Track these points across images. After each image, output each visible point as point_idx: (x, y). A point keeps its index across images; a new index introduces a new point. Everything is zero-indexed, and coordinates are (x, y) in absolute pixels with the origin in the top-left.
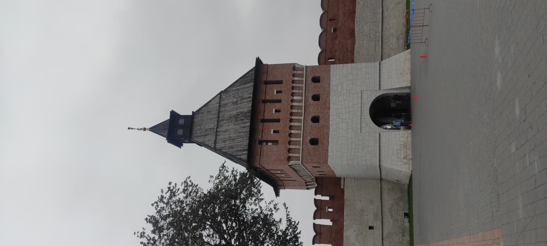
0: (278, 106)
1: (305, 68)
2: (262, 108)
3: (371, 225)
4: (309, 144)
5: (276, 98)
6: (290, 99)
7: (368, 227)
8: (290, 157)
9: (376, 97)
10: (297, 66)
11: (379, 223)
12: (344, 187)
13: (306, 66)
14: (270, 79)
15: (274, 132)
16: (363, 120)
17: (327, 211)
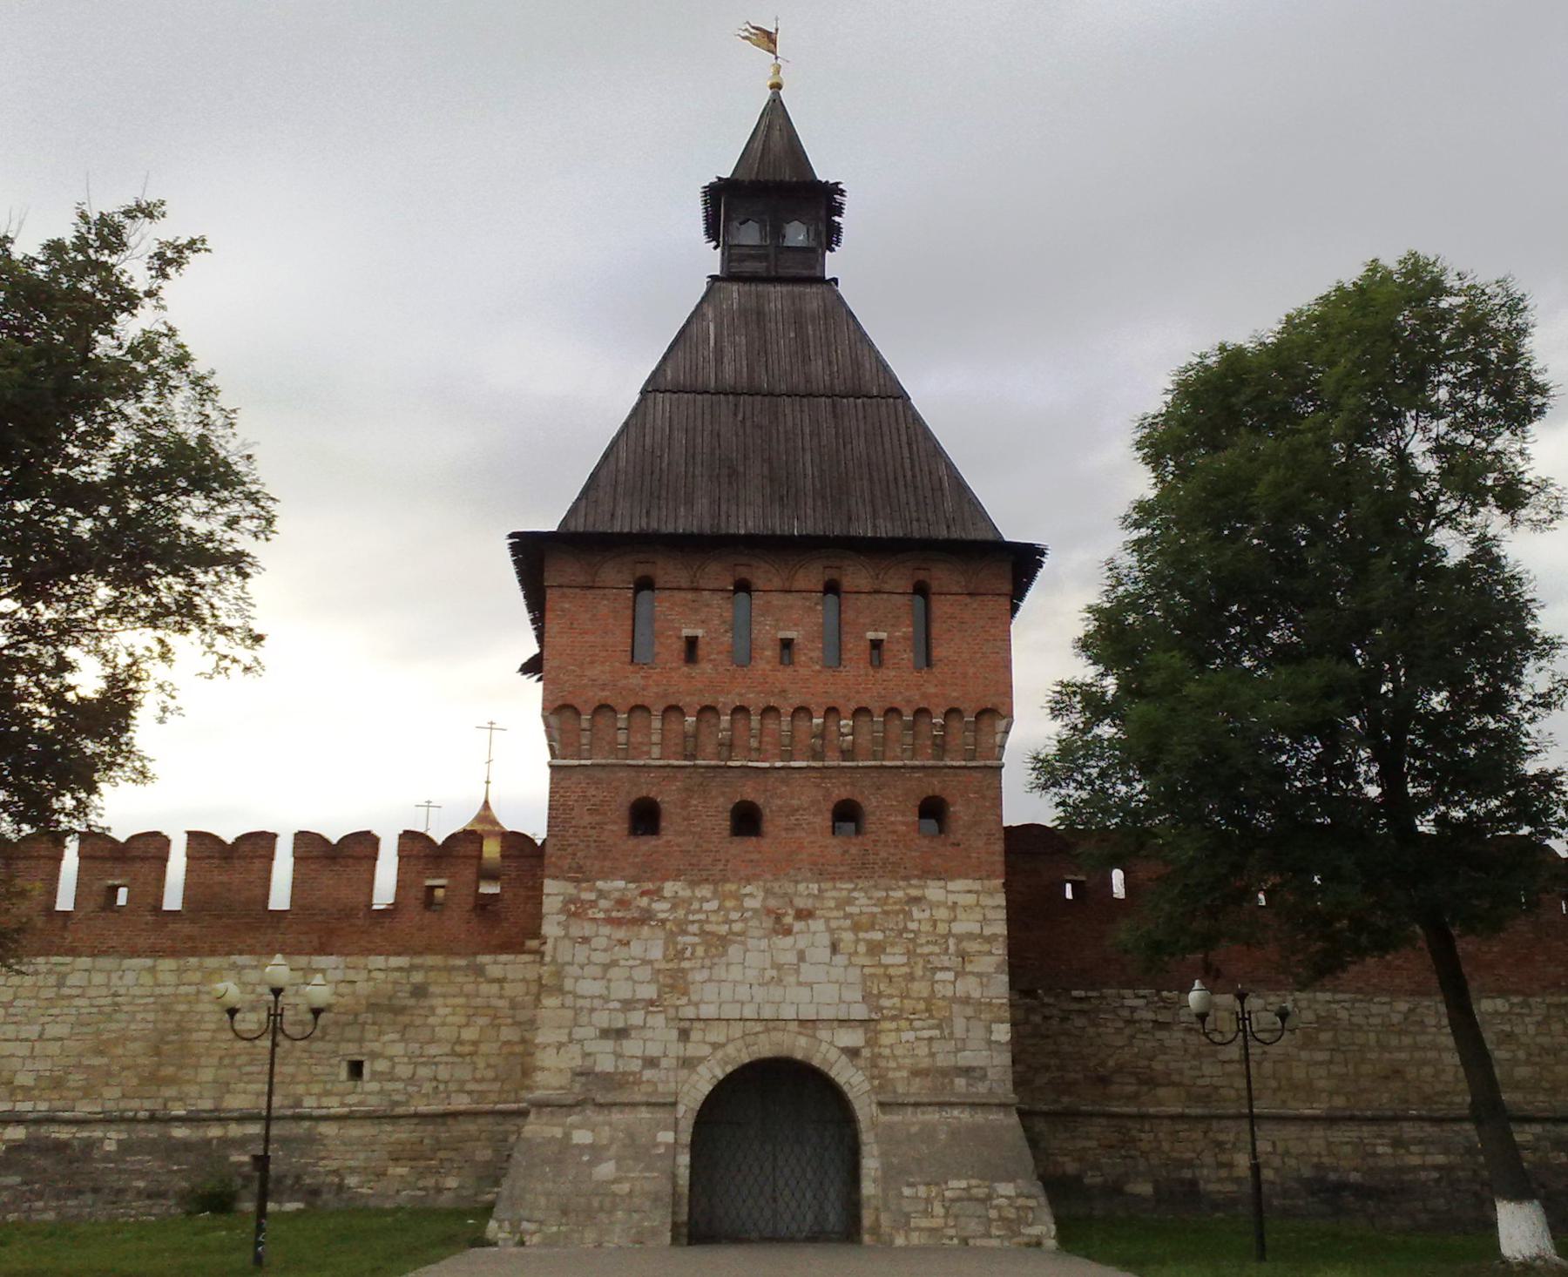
0: (810, 653)
1: (989, 763)
2: (800, 583)
3: (366, 1070)
4: (633, 797)
5: (850, 642)
6: (839, 703)
7: (359, 1058)
8: (578, 713)
9: (846, 1088)
10: (1001, 724)
11: (374, 1103)
12: (531, 952)
13: (1002, 767)
14: (940, 606)
15: (692, 642)
16: (737, 1030)
17: (429, 882)
